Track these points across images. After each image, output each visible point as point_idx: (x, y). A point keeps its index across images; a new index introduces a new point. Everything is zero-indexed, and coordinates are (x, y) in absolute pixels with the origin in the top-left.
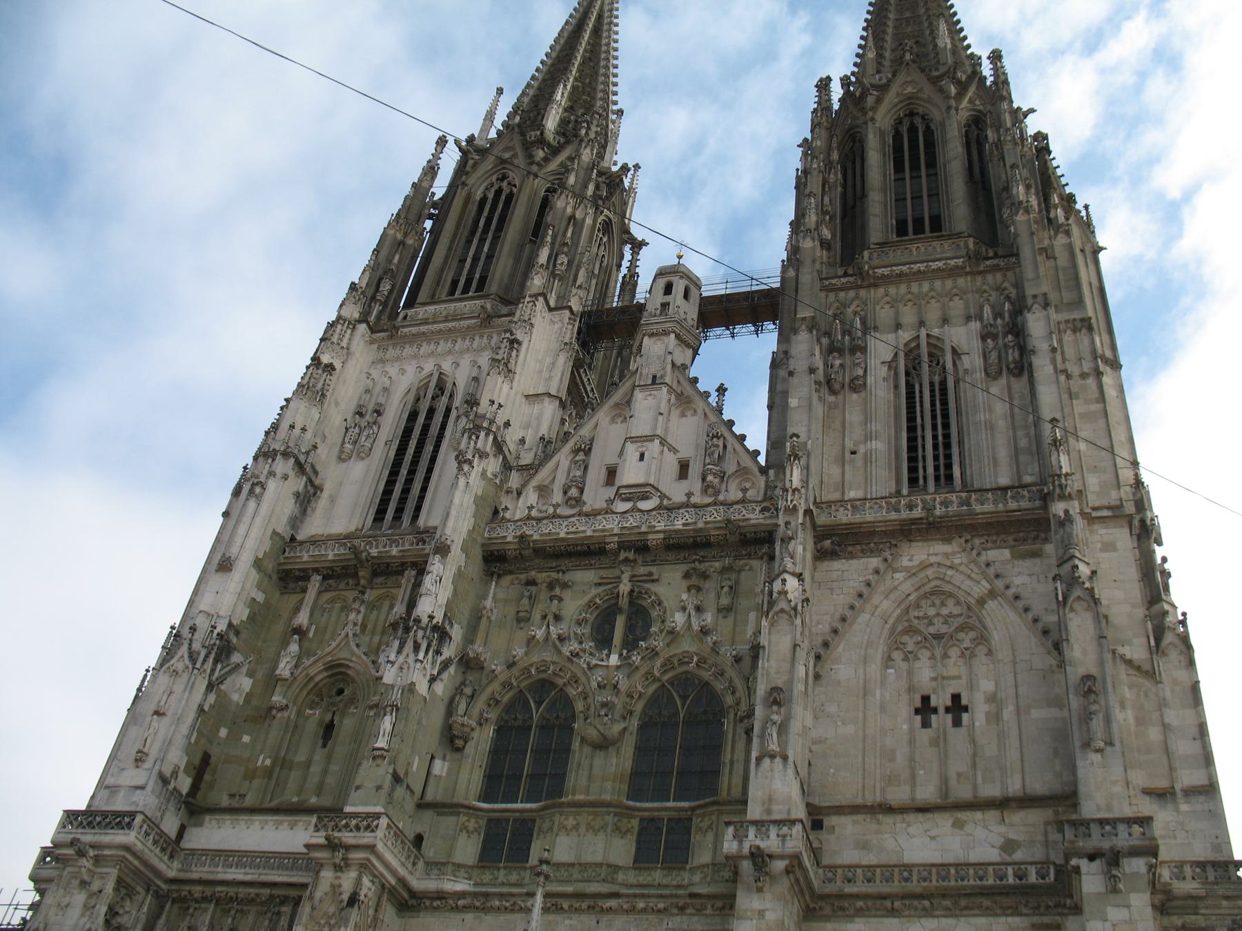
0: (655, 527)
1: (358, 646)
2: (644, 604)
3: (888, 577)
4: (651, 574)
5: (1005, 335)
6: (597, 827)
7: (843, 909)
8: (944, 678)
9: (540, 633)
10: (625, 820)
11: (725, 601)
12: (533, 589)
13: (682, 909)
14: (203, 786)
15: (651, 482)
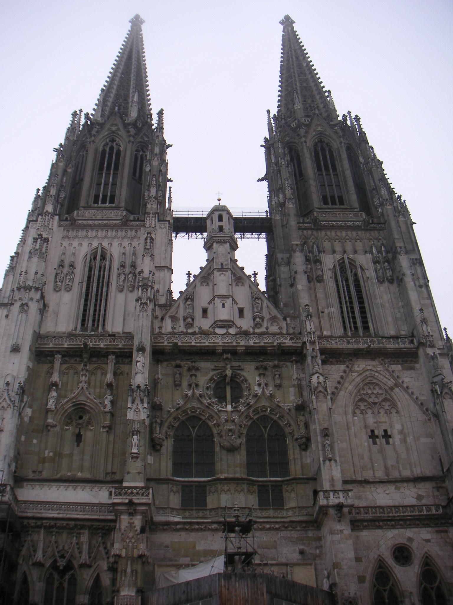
0: (240, 343)
1: (90, 394)
2: (238, 380)
3: (350, 375)
4: (240, 366)
5: (384, 263)
6: (239, 490)
7: (358, 526)
10: (251, 486)
11: (278, 382)
13: (286, 528)
15: (232, 320)
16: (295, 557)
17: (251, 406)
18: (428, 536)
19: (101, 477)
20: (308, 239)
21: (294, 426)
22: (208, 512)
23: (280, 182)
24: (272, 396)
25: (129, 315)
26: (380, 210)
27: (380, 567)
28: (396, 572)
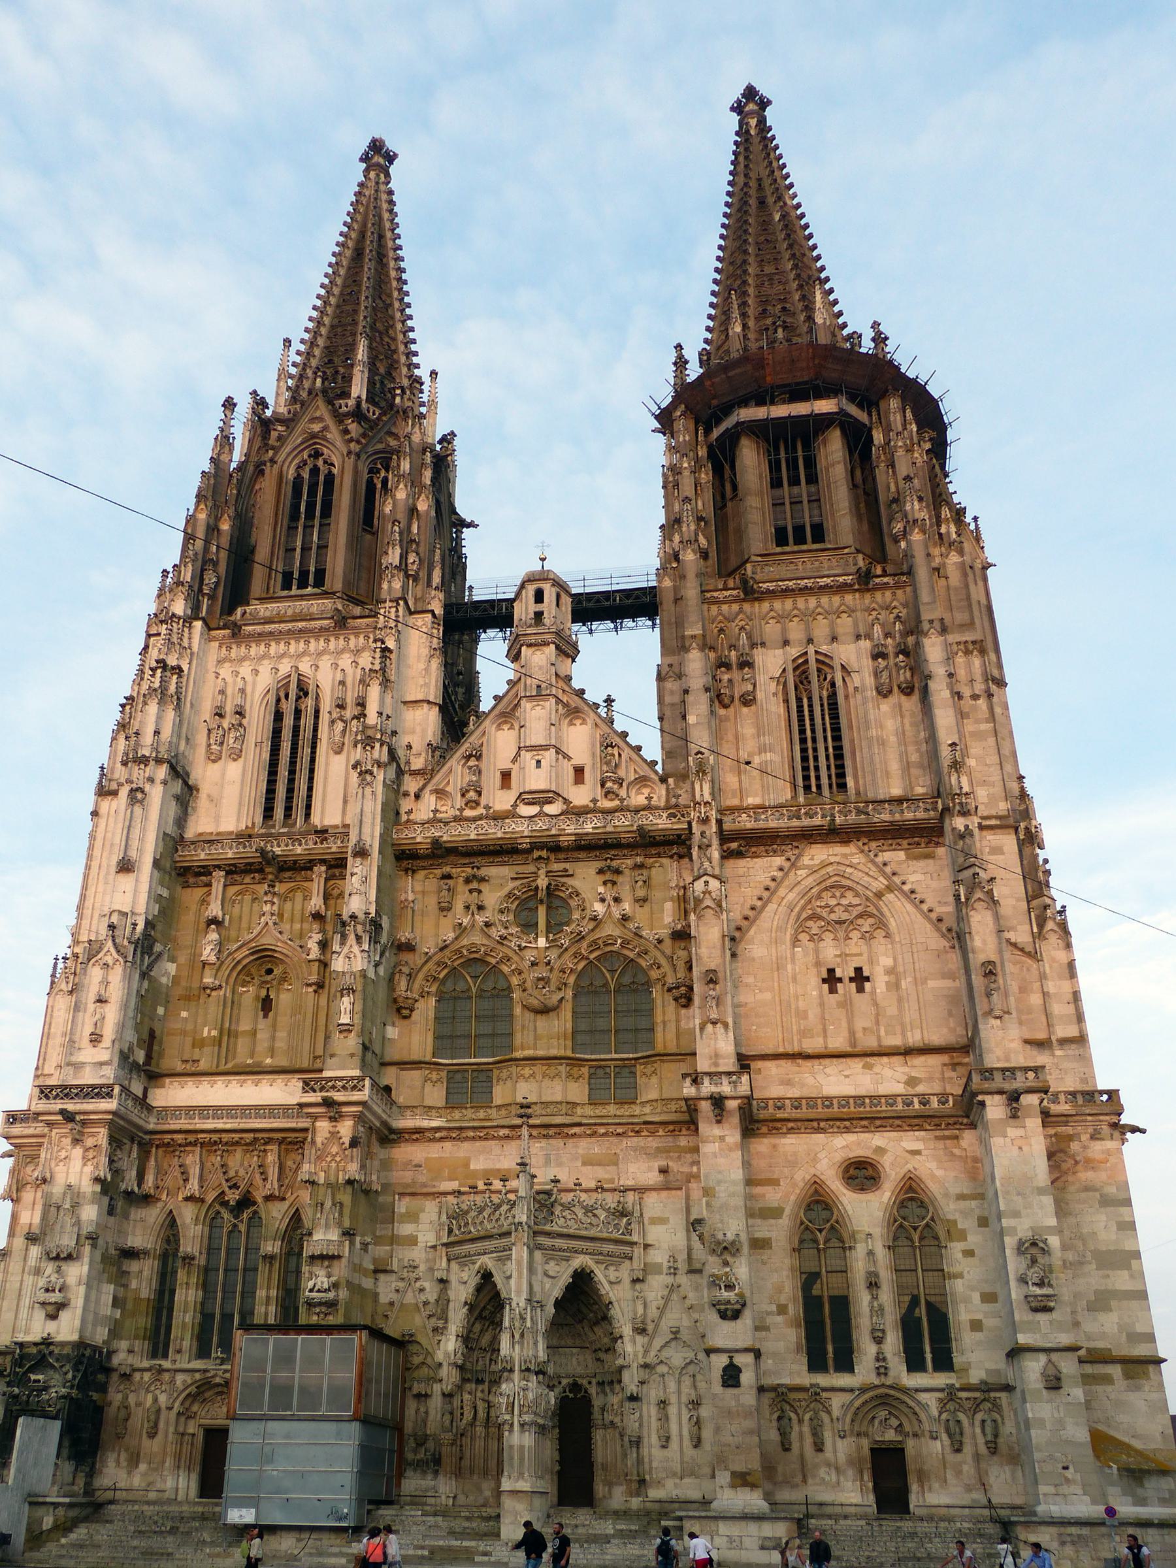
3: (792, 874)
8: (847, 955)
12: (450, 882)
14: (154, 1055)
16: (652, 1177)
18: (918, 1146)
22: (493, 1112)
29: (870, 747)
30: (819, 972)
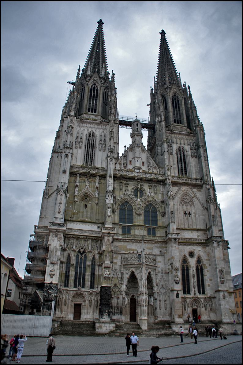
9: (126, 193)
11: (156, 192)
13: (156, 243)
16: (158, 253)
17: (146, 200)
18: (200, 249)
19: (95, 222)
20: (168, 137)
21: (160, 208)
23: (159, 112)
24: (153, 197)
25: (103, 161)
26: (194, 128)
27: (184, 258)
28: (189, 259)
29: (191, 167)
30: (183, 212)
